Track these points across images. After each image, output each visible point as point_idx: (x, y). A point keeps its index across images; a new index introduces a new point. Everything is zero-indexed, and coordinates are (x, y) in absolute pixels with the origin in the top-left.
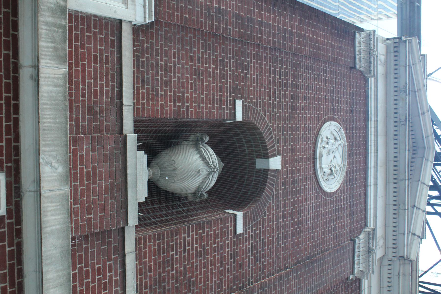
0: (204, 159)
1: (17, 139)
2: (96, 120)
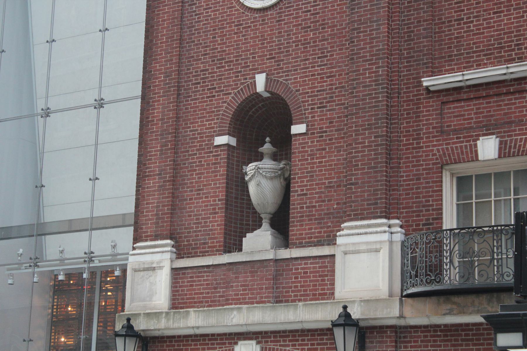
0: (250, 179)
1: (225, 334)
2: (220, 284)
